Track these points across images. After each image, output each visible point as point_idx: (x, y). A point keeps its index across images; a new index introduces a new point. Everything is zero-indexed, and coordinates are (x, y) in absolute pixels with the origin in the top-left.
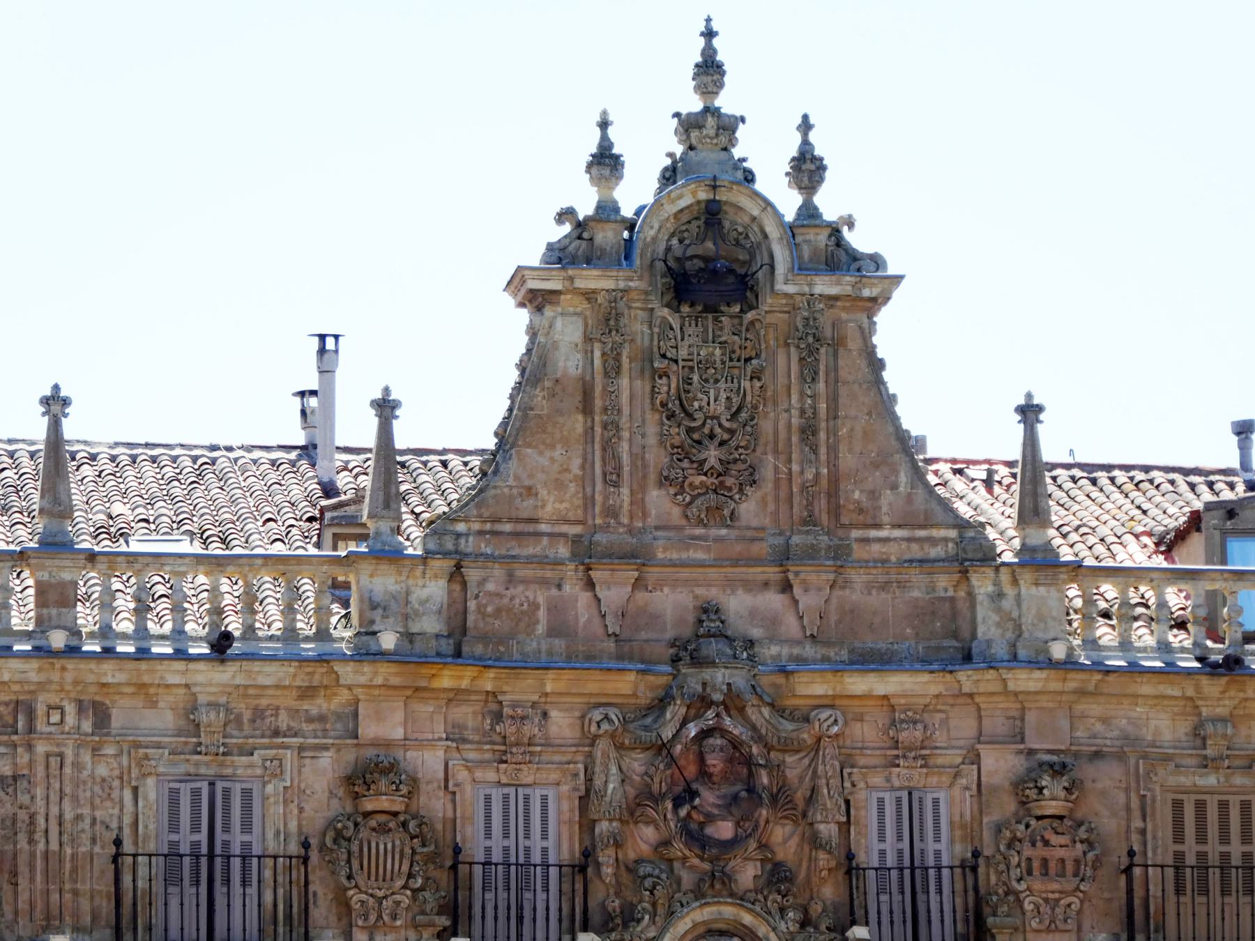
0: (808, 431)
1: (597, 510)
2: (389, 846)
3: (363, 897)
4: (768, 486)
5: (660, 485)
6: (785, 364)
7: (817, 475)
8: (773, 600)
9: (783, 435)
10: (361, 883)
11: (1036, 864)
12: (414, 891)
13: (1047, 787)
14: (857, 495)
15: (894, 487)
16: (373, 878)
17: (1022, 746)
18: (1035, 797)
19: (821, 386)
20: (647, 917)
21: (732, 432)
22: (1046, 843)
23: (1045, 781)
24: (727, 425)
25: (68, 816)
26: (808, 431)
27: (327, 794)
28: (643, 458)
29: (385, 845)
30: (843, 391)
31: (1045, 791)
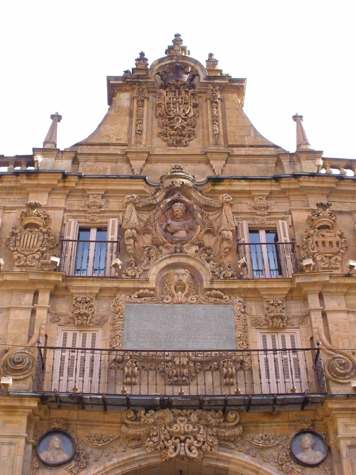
2: (33, 236)
3: (20, 255)
4: (201, 137)
5: (159, 136)
8: (203, 167)
9: (205, 123)
10: (19, 249)
11: (320, 244)
12: (43, 253)
13: (321, 213)
16: (24, 247)
17: (309, 208)
19: (220, 109)
20: (146, 261)
22: (323, 236)
28: (152, 130)
29: (32, 236)
30: (227, 111)
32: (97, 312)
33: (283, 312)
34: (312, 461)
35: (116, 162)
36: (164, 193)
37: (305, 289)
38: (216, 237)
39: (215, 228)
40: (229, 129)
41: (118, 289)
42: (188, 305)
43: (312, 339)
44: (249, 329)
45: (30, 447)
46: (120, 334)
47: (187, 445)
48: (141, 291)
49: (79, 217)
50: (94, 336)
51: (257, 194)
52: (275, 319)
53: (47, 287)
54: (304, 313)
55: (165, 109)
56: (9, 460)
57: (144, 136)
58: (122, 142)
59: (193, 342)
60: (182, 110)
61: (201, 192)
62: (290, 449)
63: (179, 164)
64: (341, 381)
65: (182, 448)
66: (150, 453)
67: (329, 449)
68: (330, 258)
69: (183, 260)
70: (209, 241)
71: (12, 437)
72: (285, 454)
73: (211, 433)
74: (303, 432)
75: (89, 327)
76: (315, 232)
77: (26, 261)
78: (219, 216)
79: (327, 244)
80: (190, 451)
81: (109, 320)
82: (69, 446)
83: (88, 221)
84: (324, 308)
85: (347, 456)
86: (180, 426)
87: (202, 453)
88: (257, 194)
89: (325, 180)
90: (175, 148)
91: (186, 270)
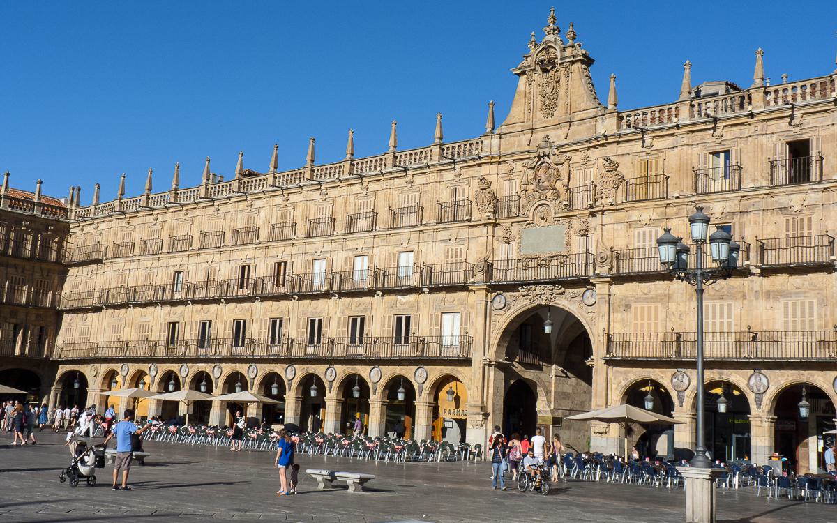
6: (563, 78)
40: (573, 98)
48: (527, 222)
58: (522, 121)
63: (547, 133)
70: (559, 185)
86: (537, 292)
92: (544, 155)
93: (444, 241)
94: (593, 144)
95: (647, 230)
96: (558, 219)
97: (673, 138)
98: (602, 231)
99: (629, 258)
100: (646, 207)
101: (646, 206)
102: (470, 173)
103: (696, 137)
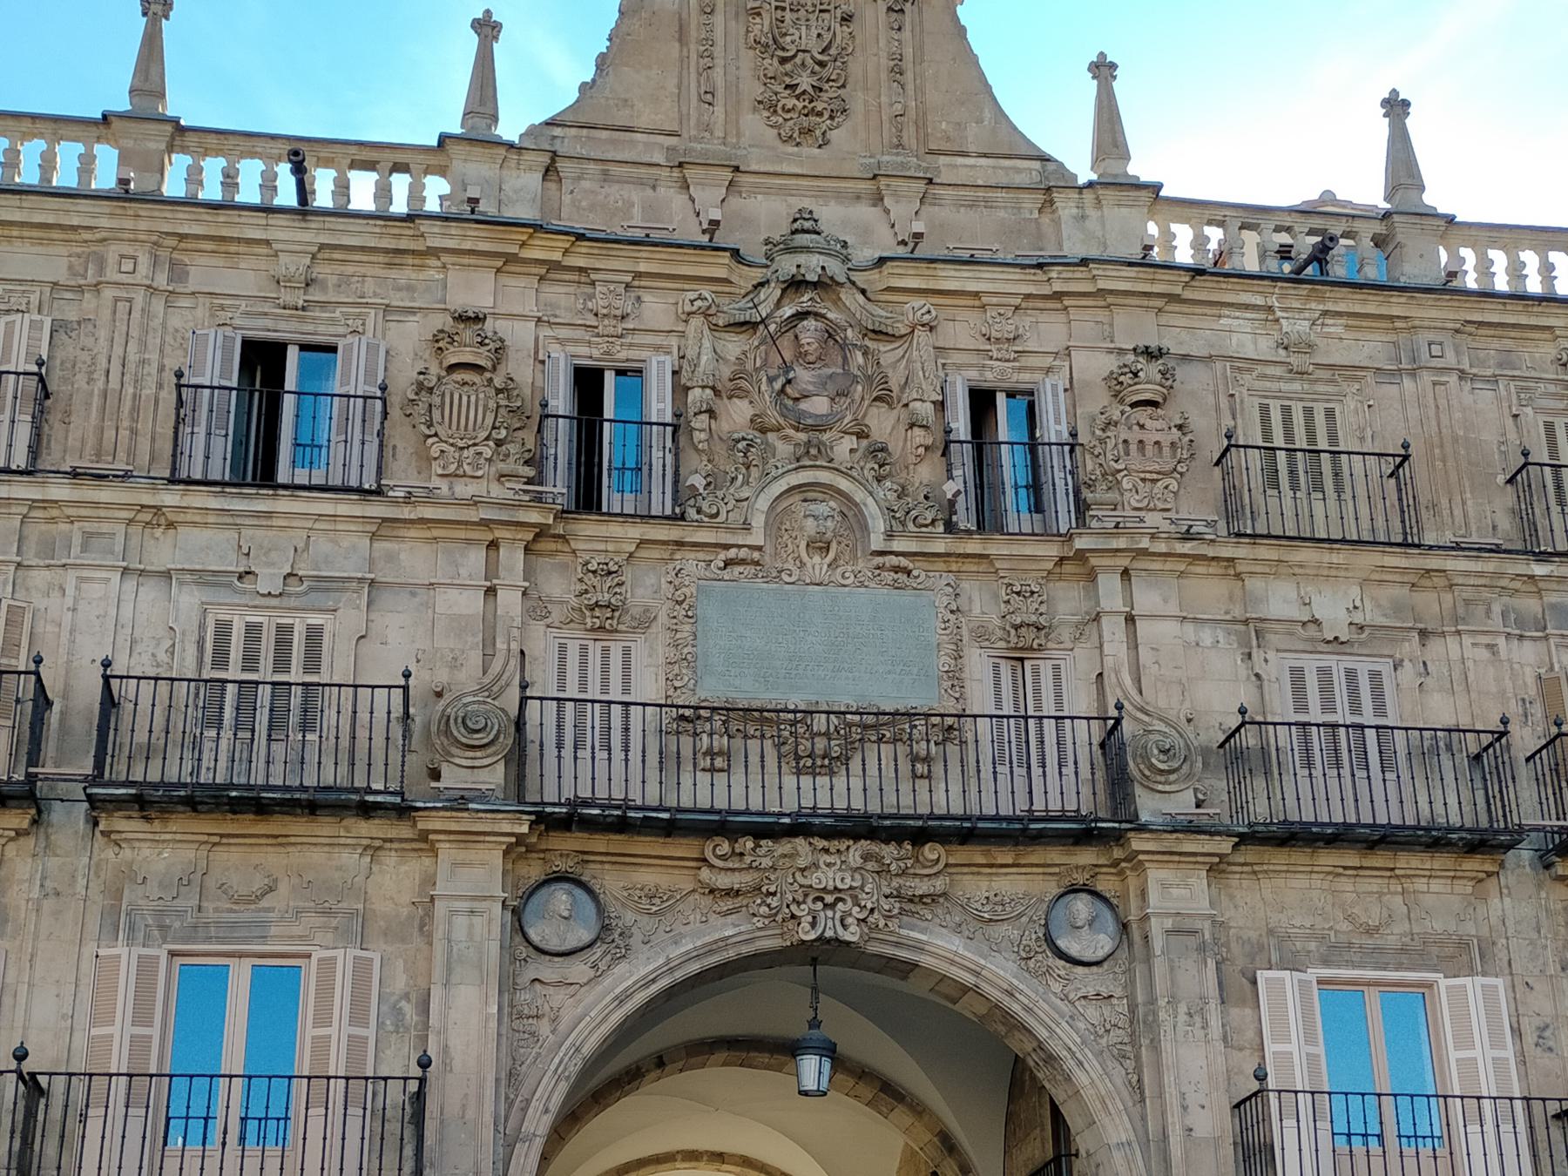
0: (897, 71)
1: (693, 122)
3: (444, 446)
5: (755, 110)
7: (905, 107)
8: (866, 212)
11: (1133, 447)
14: (944, 126)
15: (979, 121)
17: (1112, 346)
18: (1131, 382)
20: (740, 477)
21: (822, 64)
22: (1142, 427)
23: (1142, 362)
24: (820, 57)
25: (133, 357)
26: (897, 71)
27: (412, 355)
28: (737, 87)
31: (1140, 374)
32: (632, 596)
33: (1041, 614)
34: (1088, 956)
35: (654, 188)
36: (778, 292)
37: (1094, 561)
38: (895, 411)
39: (893, 388)
41: (680, 544)
42: (834, 589)
43: (1100, 674)
44: (966, 652)
45: (508, 914)
46: (689, 657)
47: (838, 915)
48: (732, 553)
49: (576, 341)
50: (627, 652)
51: (995, 300)
52: (1023, 630)
53: (519, 537)
54: (1087, 613)
55: (771, 28)
56: (471, 950)
57: (719, 110)
59: (847, 678)
60: (814, 33)
61: (863, 292)
62: (1046, 925)
63: (807, 203)
64: (1160, 787)
65: (830, 923)
66: (760, 929)
67: (1124, 927)
68: (1154, 481)
69: (824, 477)
70: (882, 423)
71: (474, 898)
72: (1034, 937)
73: (888, 891)
74: (1074, 890)
75: (617, 631)
76: (1123, 413)
77: (460, 465)
78: (903, 356)
79: (1149, 450)
80: (845, 927)
81: (660, 618)
82: (589, 908)
83: (596, 353)
84: (1132, 609)
85: (1163, 952)
86: (824, 877)
87: (866, 930)
88: (995, 300)
89: (1158, 276)
90: (796, 149)
91: (832, 504)
92: (824, 285)
93: (205, 578)
94: (1058, 287)
95: (1338, 665)
96: (904, 562)
97: (1392, 337)
98: (1134, 645)
99: (1265, 762)
100: (1329, 575)
101: (1338, 567)
102: (370, 285)
103: (1482, 354)
